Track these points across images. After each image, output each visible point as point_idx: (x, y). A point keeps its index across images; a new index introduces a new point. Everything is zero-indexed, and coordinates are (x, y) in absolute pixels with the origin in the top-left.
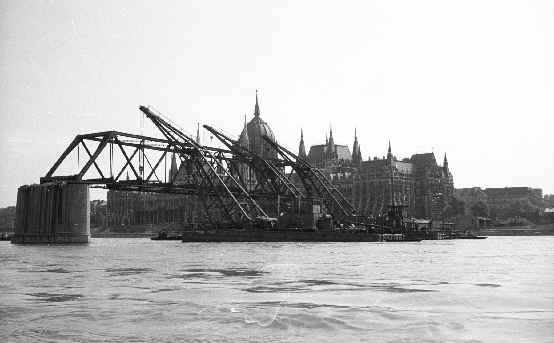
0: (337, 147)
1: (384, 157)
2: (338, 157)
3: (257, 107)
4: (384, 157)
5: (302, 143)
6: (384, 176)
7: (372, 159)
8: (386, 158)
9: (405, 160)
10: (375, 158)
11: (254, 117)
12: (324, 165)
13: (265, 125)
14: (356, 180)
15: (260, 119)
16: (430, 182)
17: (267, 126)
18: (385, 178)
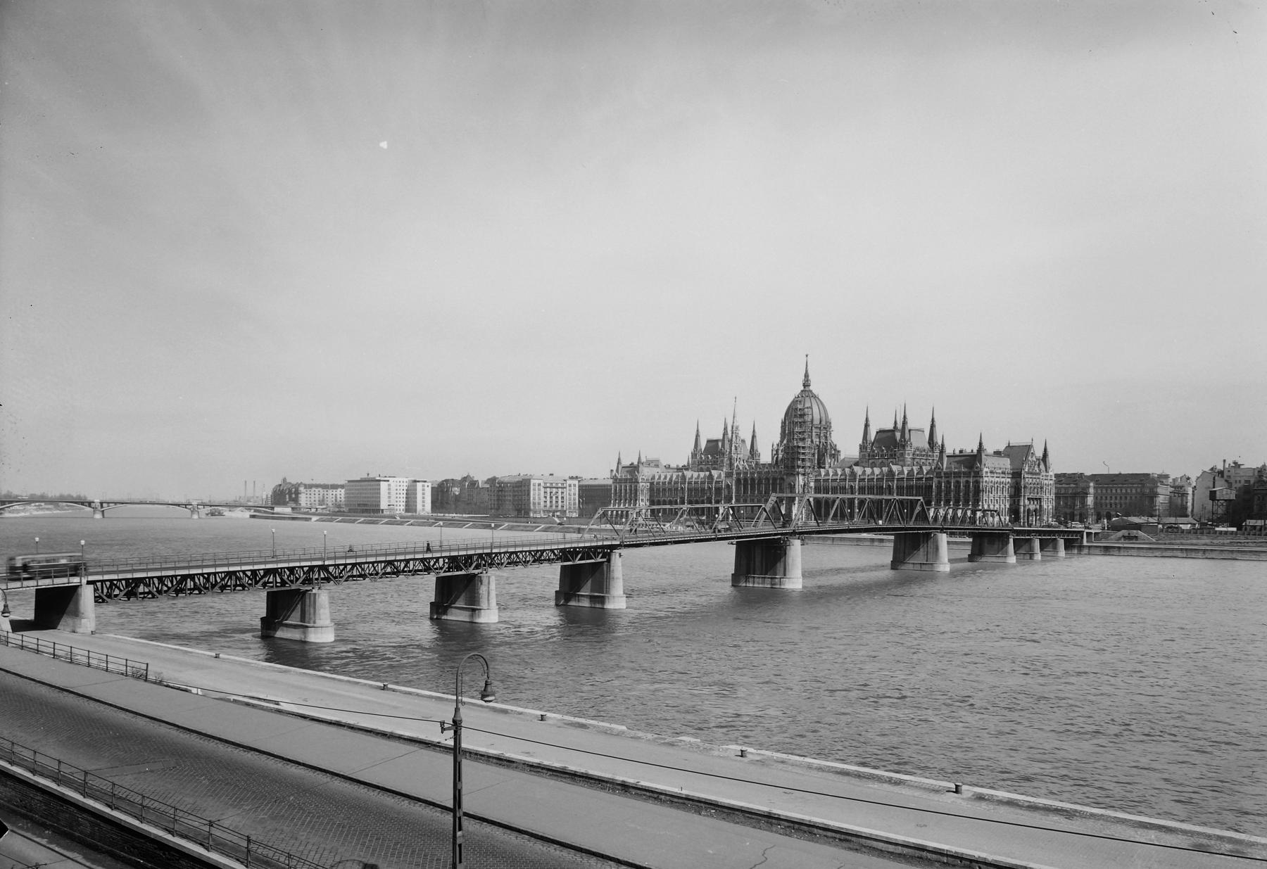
0: (911, 432)
1: (972, 451)
2: (913, 445)
3: (806, 375)
4: (972, 451)
5: (867, 426)
6: (972, 474)
7: (957, 452)
8: (975, 451)
9: (997, 453)
10: (961, 451)
11: (802, 388)
12: (895, 455)
13: (812, 398)
14: (937, 477)
15: (811, 391)
16: (1027, 480)
17: (820, 400)
18: (973, 477)
